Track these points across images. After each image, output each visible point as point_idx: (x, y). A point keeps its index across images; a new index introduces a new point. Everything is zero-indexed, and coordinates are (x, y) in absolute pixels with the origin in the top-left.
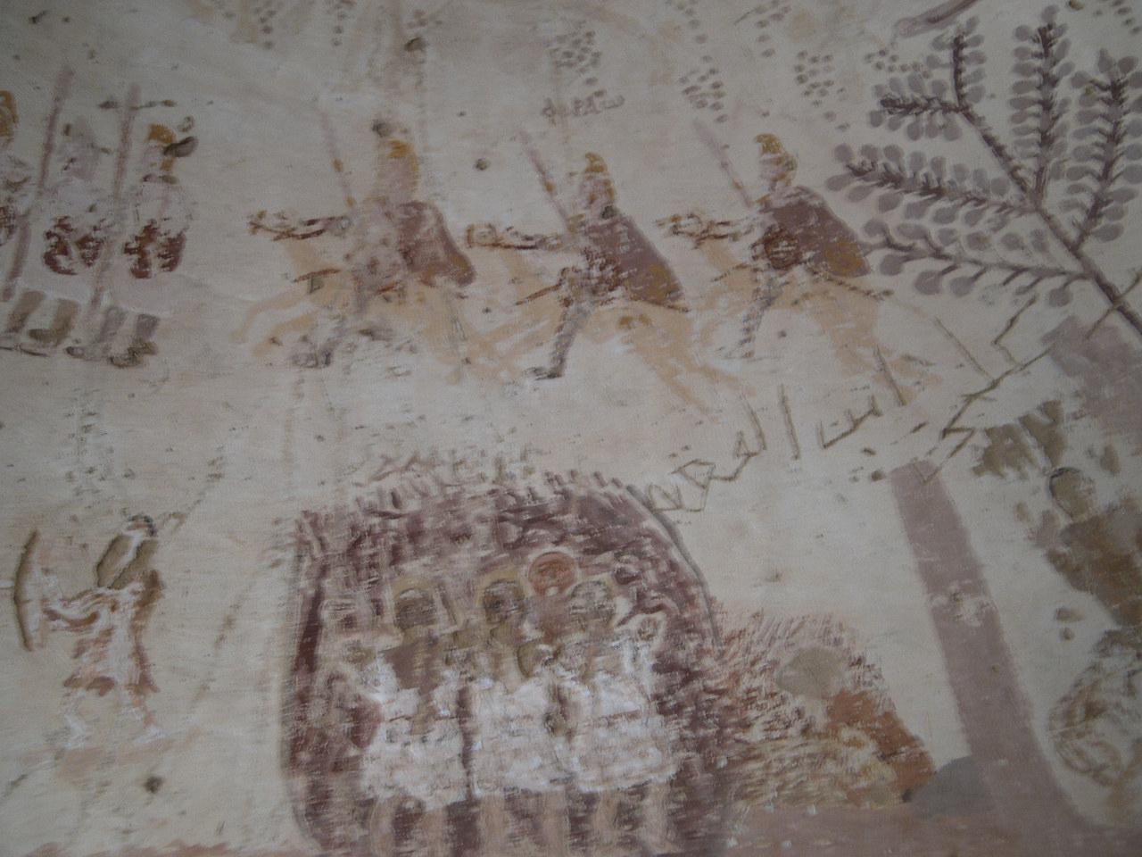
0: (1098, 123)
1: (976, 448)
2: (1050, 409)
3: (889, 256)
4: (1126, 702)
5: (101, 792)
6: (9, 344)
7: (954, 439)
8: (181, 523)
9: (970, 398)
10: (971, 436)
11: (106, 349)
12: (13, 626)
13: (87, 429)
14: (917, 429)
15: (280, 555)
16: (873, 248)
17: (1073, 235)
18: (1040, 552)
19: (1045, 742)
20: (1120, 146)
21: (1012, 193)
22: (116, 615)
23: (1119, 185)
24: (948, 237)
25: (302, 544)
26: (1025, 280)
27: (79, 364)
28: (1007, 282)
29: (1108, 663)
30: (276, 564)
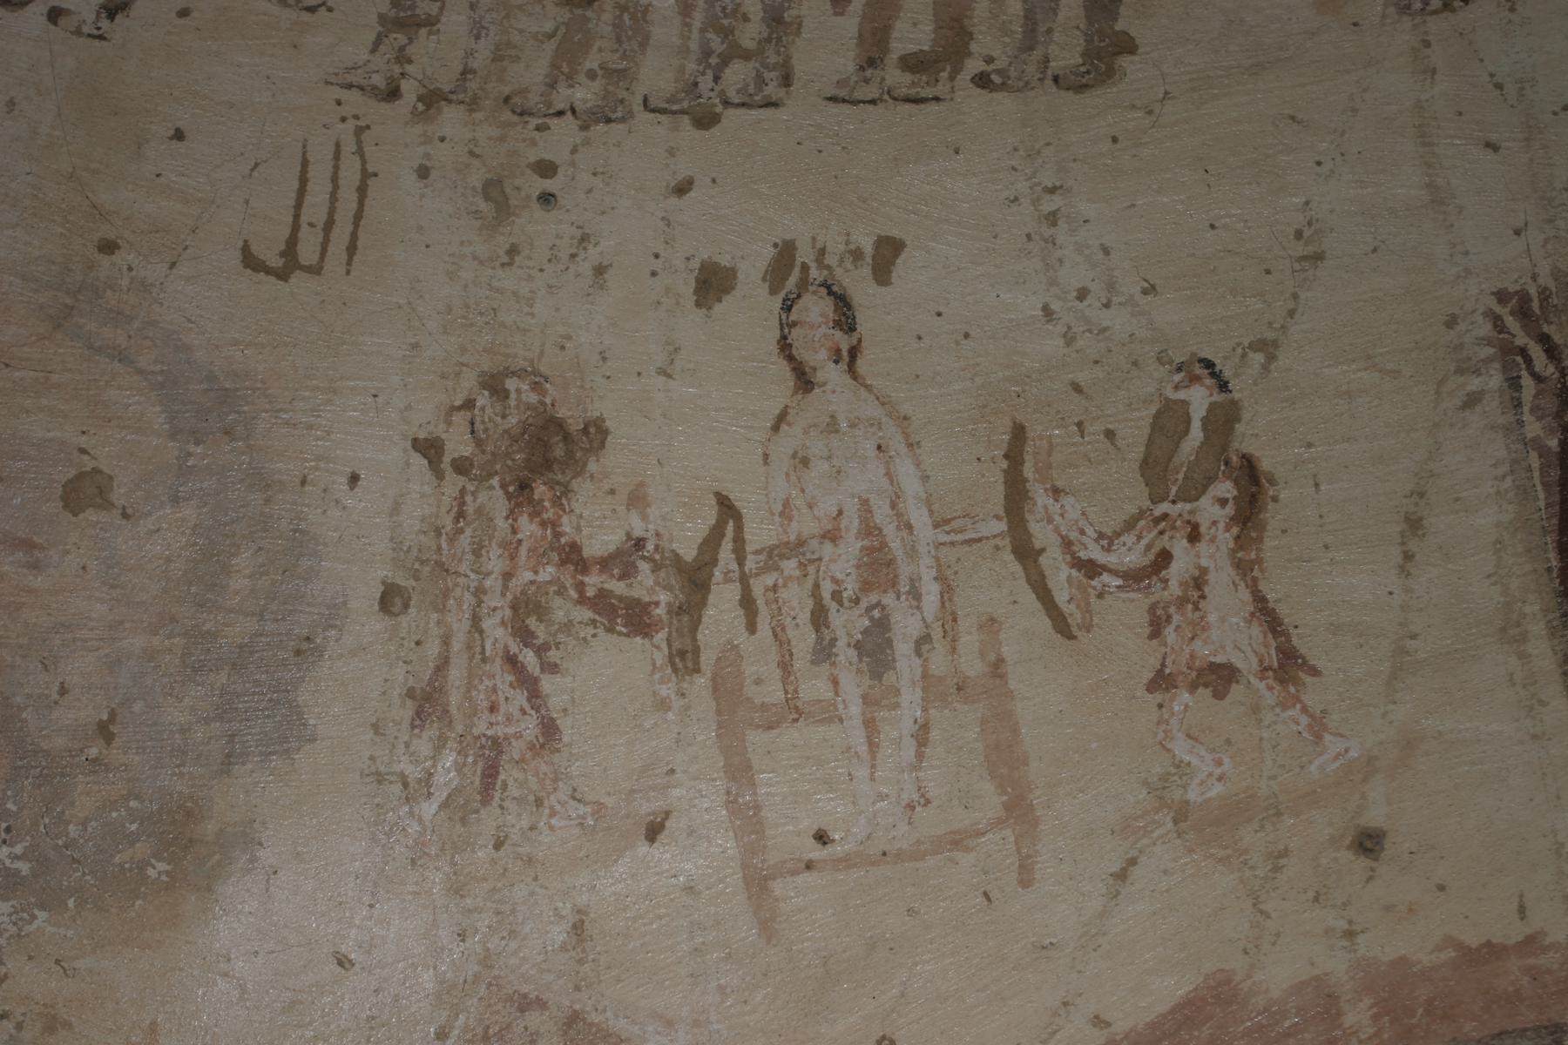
5: (1277, 869)
6: (871, 92)
8: (1271, 358)
11: (1046, 60)
12: (1029, 598)
13: (1052, 218)
15: (1474, 384)
22: (1203, 547)
25: (1510, 354)
27: (1003, 102)
30: (1472, 401)
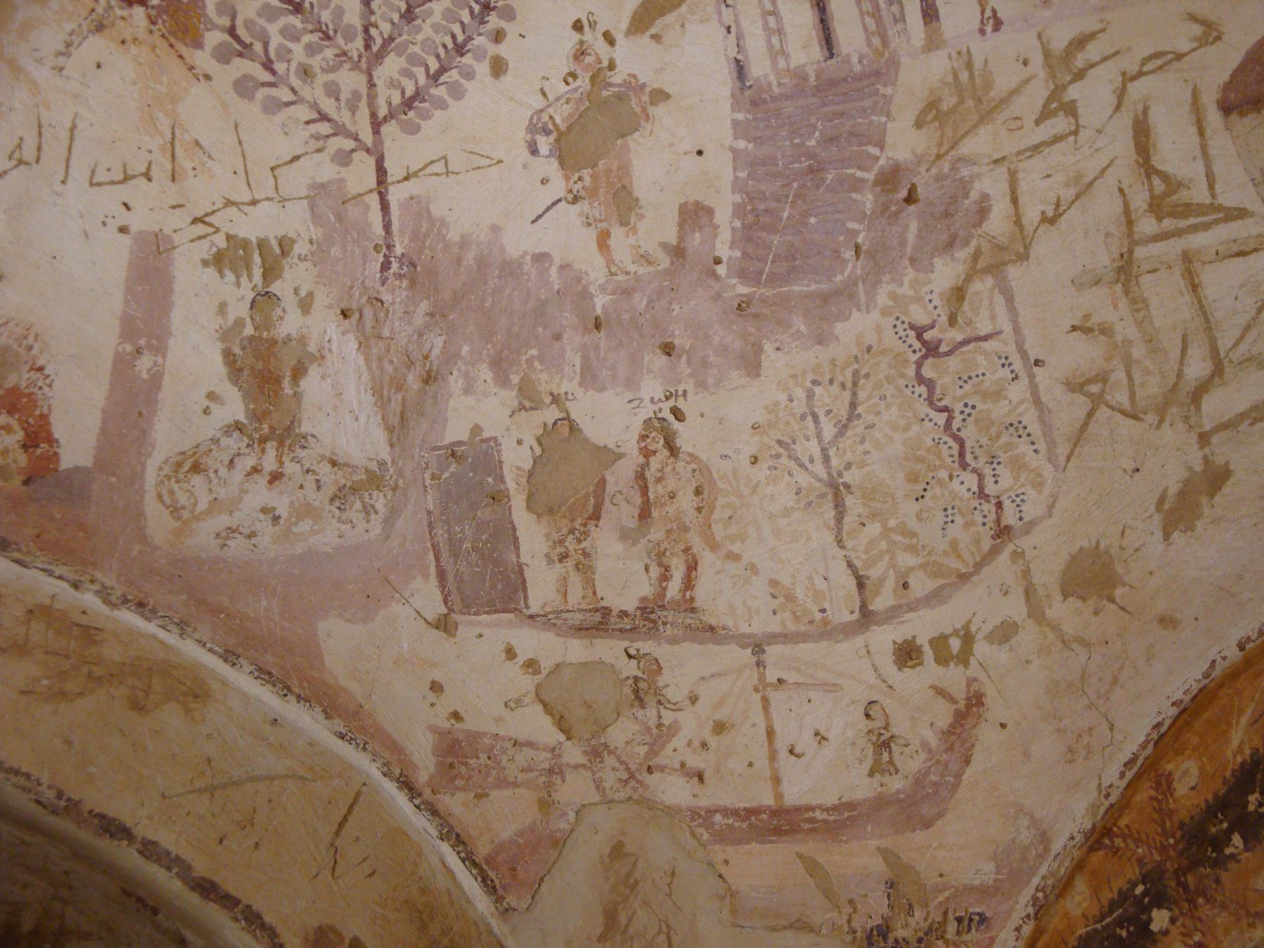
0: (457, 29)
1: (213, 244)
2: (285, 245)
3: (225, 42)
4: (223, 471)
7: (200, 229)
9: (229, 203)
10: (214, 233)
14: (174, 207)
16: (215, 27)
17: (383, 112)
18: (219, 346)
19: (150, 478)
20: (459, 59)
21: (359, 43)
23: (441, 91)
24: (285, 54)
26: (324, 128)
28: (308, 123)
29: (224, 441)
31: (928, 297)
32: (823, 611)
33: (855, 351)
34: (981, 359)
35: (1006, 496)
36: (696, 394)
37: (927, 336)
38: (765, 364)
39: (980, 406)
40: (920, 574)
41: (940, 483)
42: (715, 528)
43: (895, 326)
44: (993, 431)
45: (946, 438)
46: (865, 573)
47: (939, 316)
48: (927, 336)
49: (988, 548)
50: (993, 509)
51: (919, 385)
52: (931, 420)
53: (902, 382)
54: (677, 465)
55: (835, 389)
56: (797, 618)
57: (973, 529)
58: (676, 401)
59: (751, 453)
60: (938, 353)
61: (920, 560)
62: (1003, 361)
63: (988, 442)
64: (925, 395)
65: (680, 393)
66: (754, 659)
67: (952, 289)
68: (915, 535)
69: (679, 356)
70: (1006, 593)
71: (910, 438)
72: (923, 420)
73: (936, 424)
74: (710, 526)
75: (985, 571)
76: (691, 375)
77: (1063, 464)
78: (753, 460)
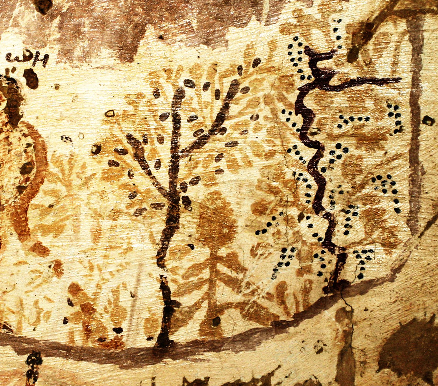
31: (335, 25)
32: (118, 330)
33: (241, 61)
34: (369, 104)
35: (351, 250)
36: (57, 63)
37: (321, 65)
38: (141, 50)
39: (353, 151)
40: (235, 313)
41: (287, 220)
42: (31, 213)
43: (290, 46)
44: (359, 179)
45: (307, 175)
46: (177, 299)
47: (340, 47)
48: (321, 65)
49: (315, 300)
50: (334, 260)
51: (297, 114)
52: (297, 153)
53: (280, 106)
54: (12, 135)
55: (208, 95)
56: (88, 331)
57: (307, 276)
58: (34, 65)
59: (94, 142)
60: (327, 85)
61: (239, 298)
62: (392, 110)
63: (350, 190)
64: (299, 125)
65: (41, 57)
66: (28, 368)
67: (362, 23)
68: (244, 270)
69: (53, 17)
70: (320, 351)
71: (270, 166)
72: (289, 150)
73: (301, 158)
74: (26, 211)
75: (305, 324)
76: (60, 40)
77: (421, 229)
78: (95, 149)
